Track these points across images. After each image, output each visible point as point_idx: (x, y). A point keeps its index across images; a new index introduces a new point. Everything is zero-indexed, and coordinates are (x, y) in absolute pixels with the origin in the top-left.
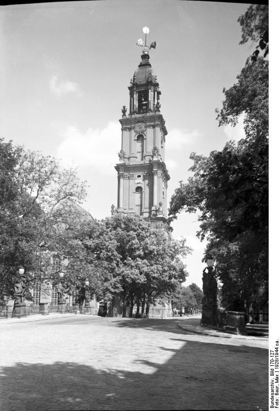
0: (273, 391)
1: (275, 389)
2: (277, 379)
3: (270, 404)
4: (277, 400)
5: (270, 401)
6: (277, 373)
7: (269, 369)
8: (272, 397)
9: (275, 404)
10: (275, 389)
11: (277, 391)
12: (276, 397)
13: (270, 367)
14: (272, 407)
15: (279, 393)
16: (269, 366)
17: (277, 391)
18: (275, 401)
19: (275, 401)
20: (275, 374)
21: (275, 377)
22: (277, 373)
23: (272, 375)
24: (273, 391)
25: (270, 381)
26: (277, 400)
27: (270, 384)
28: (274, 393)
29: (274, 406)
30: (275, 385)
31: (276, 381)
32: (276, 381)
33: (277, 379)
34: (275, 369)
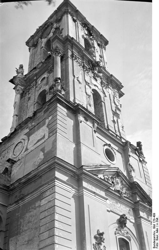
0: (155, 238)
1: (156, 237)
2: (157, 230)
6: (157, 227)
8: (154, 241)
9: (156, 246)
10: (156, 237)
11: (157, 238)
12: (156, 242)
14: (154, 248)
15: (158, 239)
16: (153, 222)
17: (157, 238)
18: (156, 244)
19: (156, 244)
20: (156, 227)
21: (156, 229)
22: (157, 227)
23: (154, 228)
24: (155, 238)
26: (157, 243)
28: (155, 239)
29: (155, 247)
30: (156, 234)
31: (156, 232)
32: (156, 232)
33: (157, 230)
34: (156, 225)
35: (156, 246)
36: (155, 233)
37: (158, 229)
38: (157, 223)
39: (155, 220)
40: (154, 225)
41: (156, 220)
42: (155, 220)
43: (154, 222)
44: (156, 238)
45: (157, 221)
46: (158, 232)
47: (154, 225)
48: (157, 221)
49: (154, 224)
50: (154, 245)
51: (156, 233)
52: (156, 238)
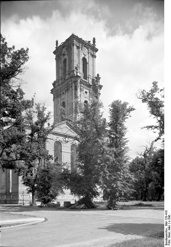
0: (167, 235)
1: (168, 234)
2: (169, 228)
3: (165, 243)
4: (169, 240)
5: (165, 241)
6: (169, 224)
7: (165, 222)
8: (166, 238)
9: (168, 243)
10: (168, 234)
11: (169, 235)
12: (168, 239)
13: (165, 221)
14: (166, 245)
16: (165, 220)
18: (168, 241)
19: (168, 241)
20: (168, 225)
21: (168, 226)
22: (169, 224)
23: (166, 225)
24: (167, 235)
25: (165, 229)
27: (165, 231)
28: (168, 236)
29: (167, 244)
30: (168, 231)
31: (169, 229)
32: (169, 229)
33: (169, 228)
34: (168, 222)
35: (168, 243)
36: (167, 230)
37: (170, 226)
38: (169, 220)
39: (167, 218)
40: (166, 222)
41: (168, 217)
42: (167, 218)
43: (166, 219)
44: (168, 235)
45: (169, 218)
46: (170, 229)
47: (166, 222)
48: (169, 218)
49: (166, 221)
50: (166, 242)
51: (168, 230)
52: (168, 235)
